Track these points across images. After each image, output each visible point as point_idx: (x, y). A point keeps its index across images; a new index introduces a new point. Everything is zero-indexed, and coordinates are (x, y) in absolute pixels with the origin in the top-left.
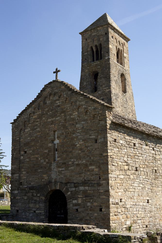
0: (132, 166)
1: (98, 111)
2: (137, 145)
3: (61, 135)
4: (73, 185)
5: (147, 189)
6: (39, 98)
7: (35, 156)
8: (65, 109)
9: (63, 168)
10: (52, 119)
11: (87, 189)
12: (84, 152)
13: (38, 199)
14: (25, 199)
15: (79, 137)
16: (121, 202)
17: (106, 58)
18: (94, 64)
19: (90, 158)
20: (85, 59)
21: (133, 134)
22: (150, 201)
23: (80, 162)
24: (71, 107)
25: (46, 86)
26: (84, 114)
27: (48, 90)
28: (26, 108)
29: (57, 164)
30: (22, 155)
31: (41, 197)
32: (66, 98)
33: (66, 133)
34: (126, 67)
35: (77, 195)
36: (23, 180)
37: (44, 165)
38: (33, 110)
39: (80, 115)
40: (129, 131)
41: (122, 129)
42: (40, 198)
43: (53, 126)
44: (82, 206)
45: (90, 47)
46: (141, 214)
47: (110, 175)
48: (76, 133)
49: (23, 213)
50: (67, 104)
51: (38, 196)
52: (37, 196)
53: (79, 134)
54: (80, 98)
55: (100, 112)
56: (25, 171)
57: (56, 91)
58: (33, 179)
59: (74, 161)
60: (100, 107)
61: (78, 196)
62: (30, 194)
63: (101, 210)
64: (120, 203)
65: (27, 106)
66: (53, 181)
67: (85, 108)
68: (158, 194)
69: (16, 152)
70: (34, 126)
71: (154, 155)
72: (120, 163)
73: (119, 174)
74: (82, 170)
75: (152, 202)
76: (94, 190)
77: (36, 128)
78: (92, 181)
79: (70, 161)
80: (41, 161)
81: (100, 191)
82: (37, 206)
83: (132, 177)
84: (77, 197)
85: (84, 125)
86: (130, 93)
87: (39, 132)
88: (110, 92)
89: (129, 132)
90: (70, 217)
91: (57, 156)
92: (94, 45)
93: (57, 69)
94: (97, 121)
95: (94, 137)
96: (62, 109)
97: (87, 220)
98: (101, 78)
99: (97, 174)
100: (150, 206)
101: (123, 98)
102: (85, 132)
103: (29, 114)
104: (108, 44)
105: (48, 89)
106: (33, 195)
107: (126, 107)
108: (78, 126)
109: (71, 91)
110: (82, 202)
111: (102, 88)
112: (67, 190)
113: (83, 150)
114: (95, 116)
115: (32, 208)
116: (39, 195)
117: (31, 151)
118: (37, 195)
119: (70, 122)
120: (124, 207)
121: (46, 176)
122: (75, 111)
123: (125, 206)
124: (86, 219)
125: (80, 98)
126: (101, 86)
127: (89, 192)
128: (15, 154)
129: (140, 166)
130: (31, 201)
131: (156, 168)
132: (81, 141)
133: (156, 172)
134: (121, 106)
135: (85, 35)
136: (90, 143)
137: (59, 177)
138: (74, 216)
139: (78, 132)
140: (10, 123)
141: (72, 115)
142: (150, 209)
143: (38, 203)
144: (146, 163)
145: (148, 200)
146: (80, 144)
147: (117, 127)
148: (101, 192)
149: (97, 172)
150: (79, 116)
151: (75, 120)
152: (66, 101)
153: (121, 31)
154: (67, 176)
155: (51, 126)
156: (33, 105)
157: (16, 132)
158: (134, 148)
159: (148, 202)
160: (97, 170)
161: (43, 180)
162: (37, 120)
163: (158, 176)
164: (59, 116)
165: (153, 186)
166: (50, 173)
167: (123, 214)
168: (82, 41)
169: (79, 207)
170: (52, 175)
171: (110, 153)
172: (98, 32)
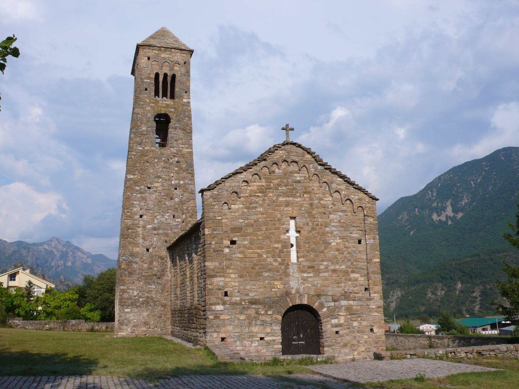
3: (304, 225)
8: (309, 189)
10: (287, 198)
12: (343, 254)
13: (268, 319)
15: (335, 233)
18: (164, 102)
19: (352, 263)
23: (337, 267)
29: (299, 268)
30: (228, 247)
31: (274, 316)
33: (313, 224)
35: (338, 312)
36: (232, 289)
37: (275, 267)
39: (336, 203)
43: (290, 209)
44: (346, 327)
45: (155, 72)
49: (236, 342)
53: (334, 229)
54: (338, 179)
56: (234, 273)
58: (254, 287)
61: (339, 313)
62: (252, 312)
63: (372, 330)
66: (294, 291)
67: (345, 196)
69: (216, 239)
70: (251, 203)
74: (341, 278)
76: (361, 305)
77: (256, 207)
78: (356, 293)
80: (268, 260)
81: (370, 307)
82: (268, 330)
87: (262, 214)
88: (191, 153)
90: (328, 343)
93: (287, 125)
96: (306, 188)
97: (354, 345)
98: (176, 128)
99: (362, 285)
105: (281, 152)
106: (257, 313)
108: (331, 216)
109: (325, 167)
112: (322, 306)
116: (270, 313)
117: (246, 242)
118: (266, 311)
124: (352, 343)
126: (176, 140)
127: (355, 307)
128: (213, 243)
130: (254, 322)
132: (338, 238)
135: (147, 50)
136: (352, 243)
137: (303, 286)
138: (333, 341)
139: (332, 226)
141: (323, 200)
146: (337, 243)
149: (362, 282)
151: (328, 208)
157: (214, 205)
162: (257, 195)
164: (300, 197)
166: (287, 279)
169: (341, 328)
170: (291, 283)
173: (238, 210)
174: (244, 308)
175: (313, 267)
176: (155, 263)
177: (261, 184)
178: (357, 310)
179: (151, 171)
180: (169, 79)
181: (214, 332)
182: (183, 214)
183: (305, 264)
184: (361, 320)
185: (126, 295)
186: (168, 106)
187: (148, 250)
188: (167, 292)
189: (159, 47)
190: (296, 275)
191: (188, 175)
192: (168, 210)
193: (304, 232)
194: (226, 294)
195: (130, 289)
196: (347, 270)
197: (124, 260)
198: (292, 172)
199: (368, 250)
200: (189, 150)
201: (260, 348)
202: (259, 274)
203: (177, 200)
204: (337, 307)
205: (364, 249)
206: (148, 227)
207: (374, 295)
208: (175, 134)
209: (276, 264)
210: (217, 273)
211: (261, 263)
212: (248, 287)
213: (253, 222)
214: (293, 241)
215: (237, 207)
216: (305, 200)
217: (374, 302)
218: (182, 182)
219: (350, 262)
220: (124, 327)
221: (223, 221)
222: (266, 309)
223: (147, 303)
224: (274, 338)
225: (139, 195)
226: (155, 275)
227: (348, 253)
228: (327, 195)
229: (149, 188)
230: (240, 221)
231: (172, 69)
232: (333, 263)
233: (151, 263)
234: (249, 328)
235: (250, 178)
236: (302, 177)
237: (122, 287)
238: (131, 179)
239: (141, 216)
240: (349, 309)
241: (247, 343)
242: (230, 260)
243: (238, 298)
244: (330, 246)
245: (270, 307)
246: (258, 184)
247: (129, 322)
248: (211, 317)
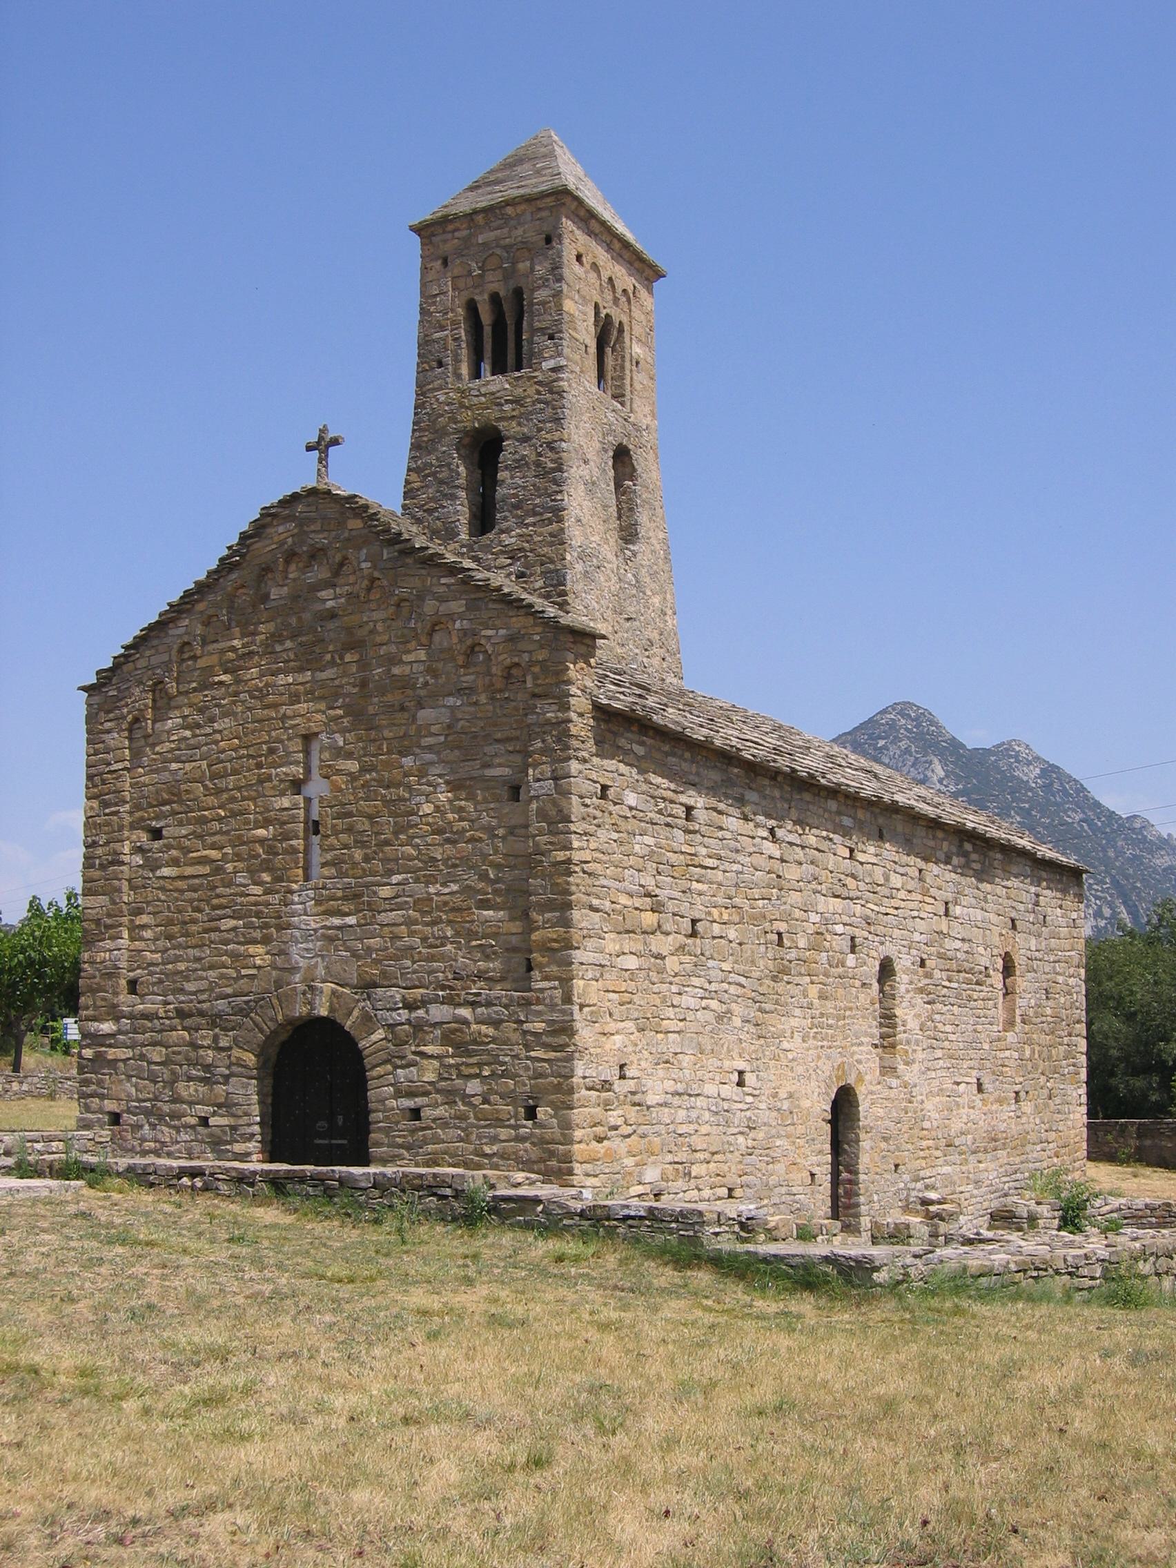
0: (674, 914)
1: (531, 647)
2: (701, 815)
4: (398, 997)
5: (737, 1022)
6: (231, 570)
9: (347, 915)
16: (622, 1077)
17: (546, 365)
20: (434, 364)
21: (684, 764)
22: (750, 1078)
24: (394, 623)
25: (268, 517)
26: (461, 660)
27: (282, 531)
28: (160, 615)
30: (139, 850)
31: (236, 1052)
32: (373, 580)
34: (642, 413)
35: (418, 1045)
38: (199, 630)
40: (667, 748)
41: (636, 737)
42: (229, 1057)
46: (707, 1134)
47: (578, 955)
48: (417, 751)
50: (373, 606)
51: (221, 1045)
54: (443, 581)
55: (541, 656)
57: (322, 539)
58: (197, 966)
60: (539, 629)
63: (531, 1114)
64: (618, 1086)
65: (169, 604)
67: (464, 633)
68: (785, 1045)
71: (776, 865)
72: (623, 900)
73: (617, 947)
75: (759, 1085)
83: (672, 964)
84: (414, 1053)
86: (658, 547)
88: (559, 539)
89: (667, 754)
91: (317, 857)
92: (486, 297)
93: (323, 431)
94: (520, 696)
95: (507, 771)
96: (349, 630)
99: (515, 950)
100: (749, 1099)
101: (622, 571)
102: (458, 748)
103: (176, 647)
104: (558, 294)
105: (281, 529)
107: (634, 616)
108: (425, 715)
109: (397, 547)
112: (368, 1021)
114: (514, 671)
118: (216, 1038)
119: (389, 698)
120: (635, 1104)
122: (414, 643)
123: (637, 1098)
125: (443, 581)
129: (709, 913)
131: (782, 927)
133: (780, 943)
134: (609, 612)
140: (79, 689)
141: (401, 662)
142: (748, 1113)
144: (737, 901)
145: (741, 1073)
147: (615, 728)
148: (535, 1034)
149: (514, 940)
150: (431, 671)
151: (414, 688)
152: (369, 590)
153: (620, 227)
155: (289, 713)
156: (197, 601)
158: (688, 831)
159: (741, 1084)
160: (514, 931)
161: (244, 972)
163: (790, 962)
164: (333, 663)
165: (767, 1007)
167: (629, 1136)
168: (424, 269)
169: (425, 1100)
171: (582, 849)
172: (506, 230)
175: (357, 896)
180: (506, 307)
189: (466, 215)
198: (315, 588)
201: (197, 1147)
204: (418, 1027)
209: (257, 890)
212: (182, 966)
216: (345, 674)
230: (174, 766)
231: (508, 275)
232: (417, 880)
236: (341, 596)
240: (454, 1037)
241: (166, 1133)
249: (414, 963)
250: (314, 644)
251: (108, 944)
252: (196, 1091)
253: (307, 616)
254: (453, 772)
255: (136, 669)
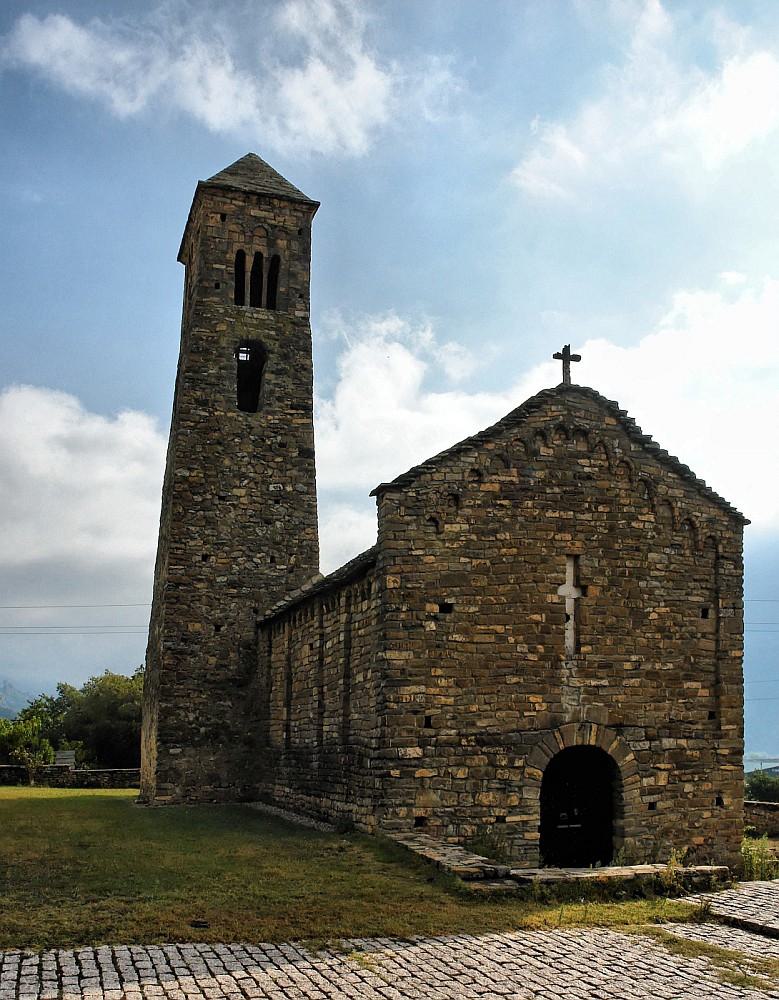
7: (491, 627)
9: (602, 678)
10: (562, 513)
11: (686, 746)
12: (670, 638)
13: (516, 778)
14: (458, 776)
15: (657, 592)
19: (687, 659)
30: (435, 618)
35: (654, 764)
37: (531, 663)
43: (568, 537)
48: (648, 578)
49: (447, 826)
52: (511, 766)
53: (655, 583)
58: (487, 707)
59: (639, 663)
61: (658, 765)
62: (480, 761)
66: (567, 718)
70: (486, 523)
77: (495, 532)
78: (690, 722)
79: (628, 661)
81: (719, 751)
82: (514, 800)
84: (653, 768)
85: (673, 561)
96: (601, 490)
99: (704, 706)
106: (492, 764)
110: (668, 783)
111: (282, 407)
112: (624, 749)
113: (667, 633)
115: (490, 806)
117: (473, 609)
118: (511, 761)
121: (541, 700)
126: (279, 399)
130: (485, 782)
132: (662, 604)
138: (643, 823)
143: (516, 789)
146: (659, 614)
148: (724, 756)
149: (704, 700)
154: (614, 707)
155: (557, 537)
161: (526, 714)
162: (499, 502)
164: (589, 510)
166: (557, 691)
173: (457, 537)
174: (466, 754)
176: (232, 655)
177: (508, 479)
178: (691, 759)
179: (227, 462)
181: (400, 805)
182: (291, 555)
183: (597, 658)
184: (700, 779)
185: (172, 721)
186: (262, 324)
187: (218, 628)
188: (256, 714)
190: (575, 682)
191: (301, 473)
192: (260, 545)
193: (593, 591)
194: (428, 724)
195: (179, 708)
196: (677, 674)
197: (169, 649)
199: (722, 631)
200: (305, 421)
202: (498, 678)
203: (278, 524)
204: (656, 753)
205: (710, 629)
206: (219, 579)
207: (727, 727)
208: (276, 385)
209: (531, 657)
210: (410, 675)
211: (502, 654)
212: (474, 708)
213: (488, 564)
214: (569, 608)
215: (456, 528)
217: (727, 743)
218: (289, 489)
219: (683, 657)
220: (169, 786)
221: (427, 559)
222: (511, 755)
223: (214, 736)
224: (525, 818)
225: (202, 512)
226: (234, 681)
227: (681, 638)
228: (645, 510)
229: (221, 498)
230: (463, 560)
232: (648, 660)
233: (224, 656)
234: (474, 797)
235: (487, 464)
237: (164, 705)
238: (185, 479)
239: (205, 558)
242: (438, 646)
243: (453, 732)
244: (646, 621)
245: (520, 753)
246: (502, 478)
247: (178, 774)
248: (395, 773)
249: (645, 711)
250: (575, 493)
251: (414, 689)
252: (494, 797)
253: (569, 473)
254: (669, 594)
255: (432, 480)
